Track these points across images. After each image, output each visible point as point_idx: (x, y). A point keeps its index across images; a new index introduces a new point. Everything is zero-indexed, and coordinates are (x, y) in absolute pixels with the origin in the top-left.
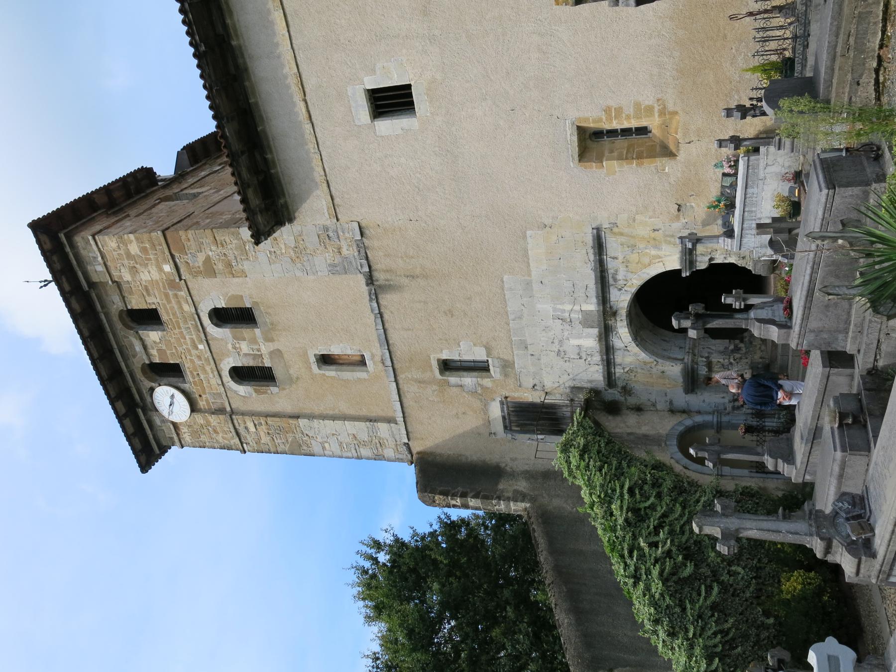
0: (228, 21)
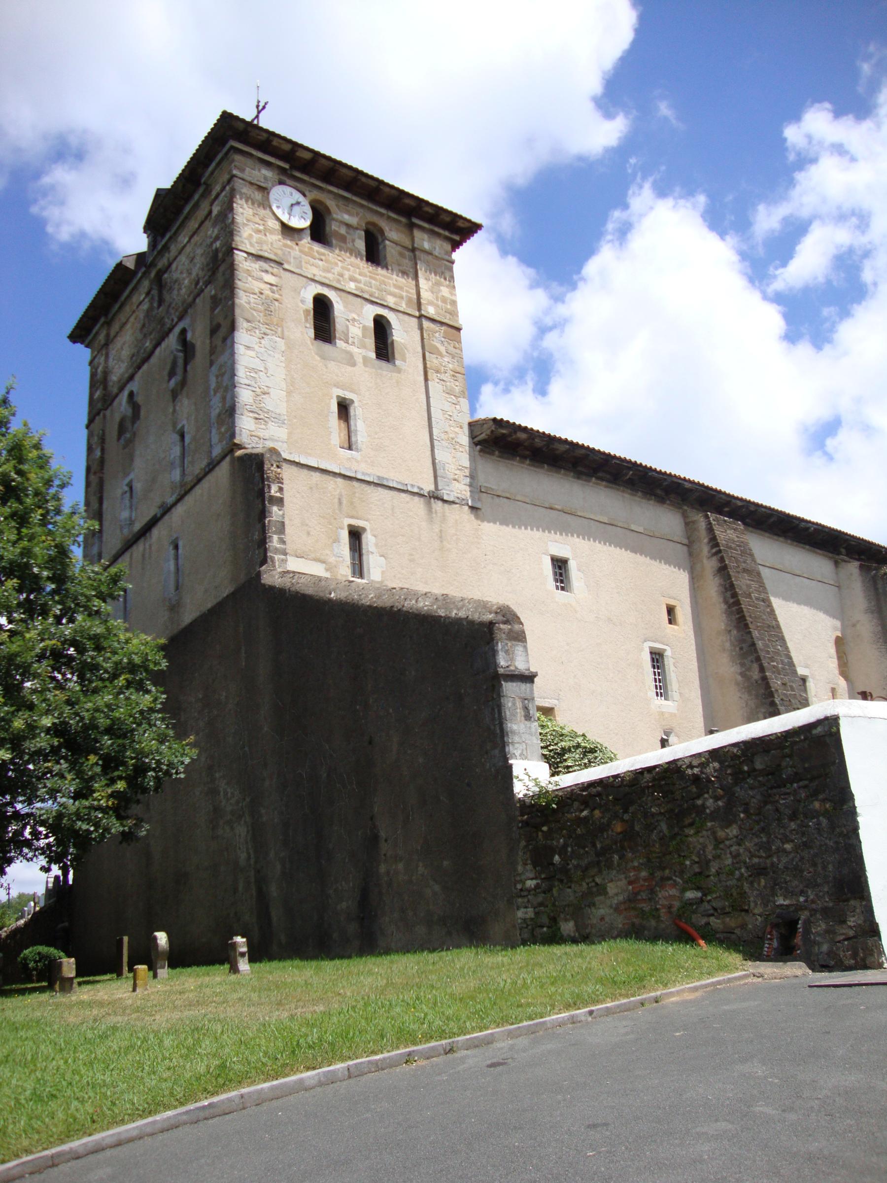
0: (604, 483)
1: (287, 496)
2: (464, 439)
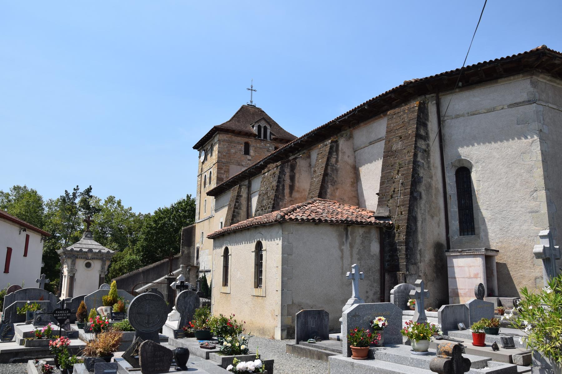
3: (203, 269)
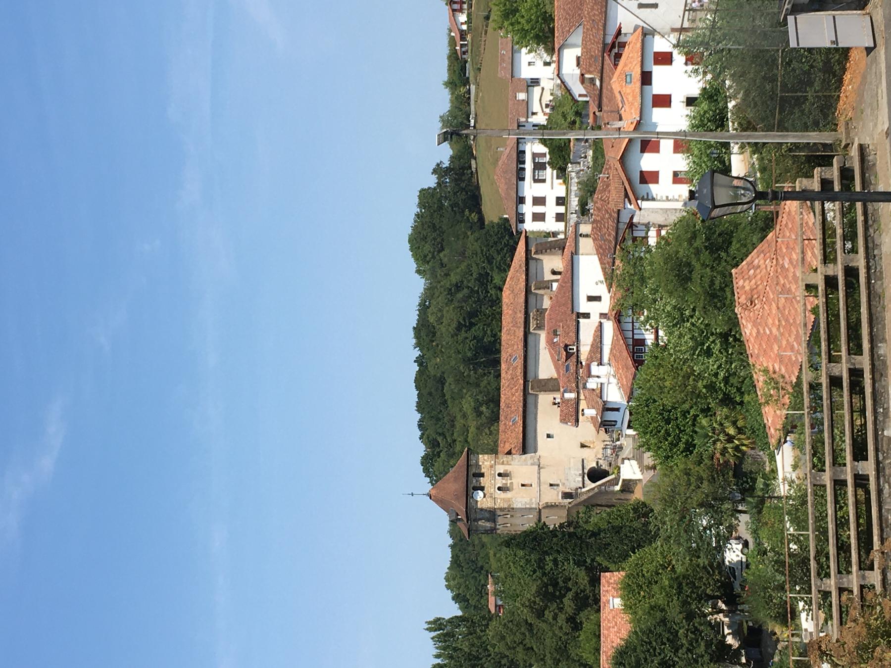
1: (554, 501)
2: (524, 457)
3: (580, 479)
